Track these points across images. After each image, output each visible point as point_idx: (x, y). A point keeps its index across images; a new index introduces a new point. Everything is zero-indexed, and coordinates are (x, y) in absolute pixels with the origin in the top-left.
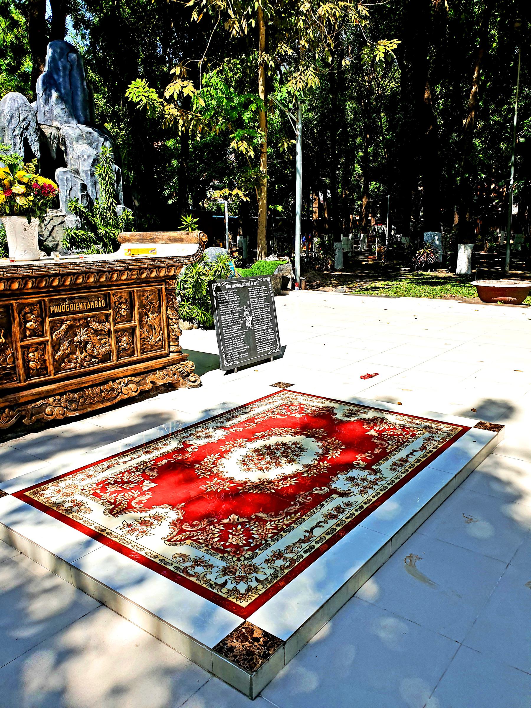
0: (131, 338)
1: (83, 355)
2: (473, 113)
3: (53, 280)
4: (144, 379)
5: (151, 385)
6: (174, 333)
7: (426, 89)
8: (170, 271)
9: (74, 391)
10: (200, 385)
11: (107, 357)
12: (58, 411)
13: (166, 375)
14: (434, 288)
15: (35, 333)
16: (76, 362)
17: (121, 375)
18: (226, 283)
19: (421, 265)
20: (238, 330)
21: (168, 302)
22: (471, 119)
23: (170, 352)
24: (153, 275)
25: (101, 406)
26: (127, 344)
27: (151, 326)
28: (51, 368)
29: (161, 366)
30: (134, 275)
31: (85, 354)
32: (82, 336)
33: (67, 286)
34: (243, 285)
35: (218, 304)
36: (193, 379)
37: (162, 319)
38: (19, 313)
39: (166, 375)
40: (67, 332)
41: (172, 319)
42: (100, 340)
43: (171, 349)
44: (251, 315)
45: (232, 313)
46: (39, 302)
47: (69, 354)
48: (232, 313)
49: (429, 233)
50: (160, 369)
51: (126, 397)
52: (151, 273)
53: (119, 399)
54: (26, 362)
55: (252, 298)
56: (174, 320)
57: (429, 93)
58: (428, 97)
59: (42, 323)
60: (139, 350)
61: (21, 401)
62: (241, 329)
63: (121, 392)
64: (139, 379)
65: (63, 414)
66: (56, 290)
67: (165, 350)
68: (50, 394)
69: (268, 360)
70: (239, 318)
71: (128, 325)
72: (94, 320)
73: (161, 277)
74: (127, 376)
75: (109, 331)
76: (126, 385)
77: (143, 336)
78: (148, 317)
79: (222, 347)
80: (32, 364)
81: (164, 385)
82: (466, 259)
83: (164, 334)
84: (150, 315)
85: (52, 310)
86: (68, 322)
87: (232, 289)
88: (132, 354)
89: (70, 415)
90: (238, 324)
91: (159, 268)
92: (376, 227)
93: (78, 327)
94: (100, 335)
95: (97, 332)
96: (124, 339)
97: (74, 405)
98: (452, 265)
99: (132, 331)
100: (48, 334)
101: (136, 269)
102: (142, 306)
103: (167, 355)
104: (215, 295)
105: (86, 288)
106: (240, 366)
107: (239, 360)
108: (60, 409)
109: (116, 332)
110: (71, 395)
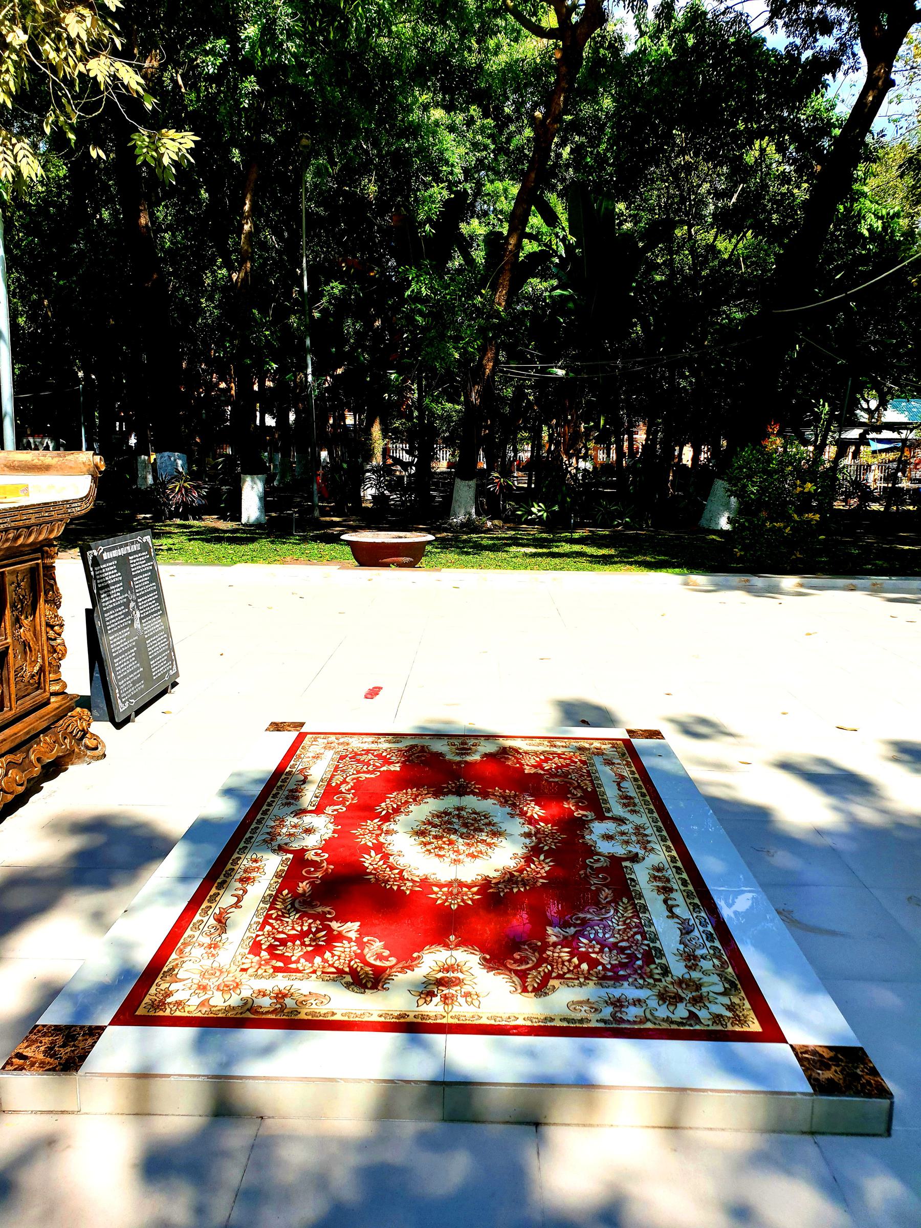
2: (249, 265)
4: (27, 756)
7: (141, 211)
10: (104, 755)
14: (251, 546)
19: (177, 508)
21: (46, 594)
22: (246, 273)
37: (38, 628)
41: (52, 627)
49: (166, 454)
50: (45, 731)
56: (56, 628)
57: (147, 217)
58: (147, 224)
60: (13, 696)
67: (45, 691)
76: (6, 774)
82: (257, 500)
92: (31, 440)
98: (233, 509)
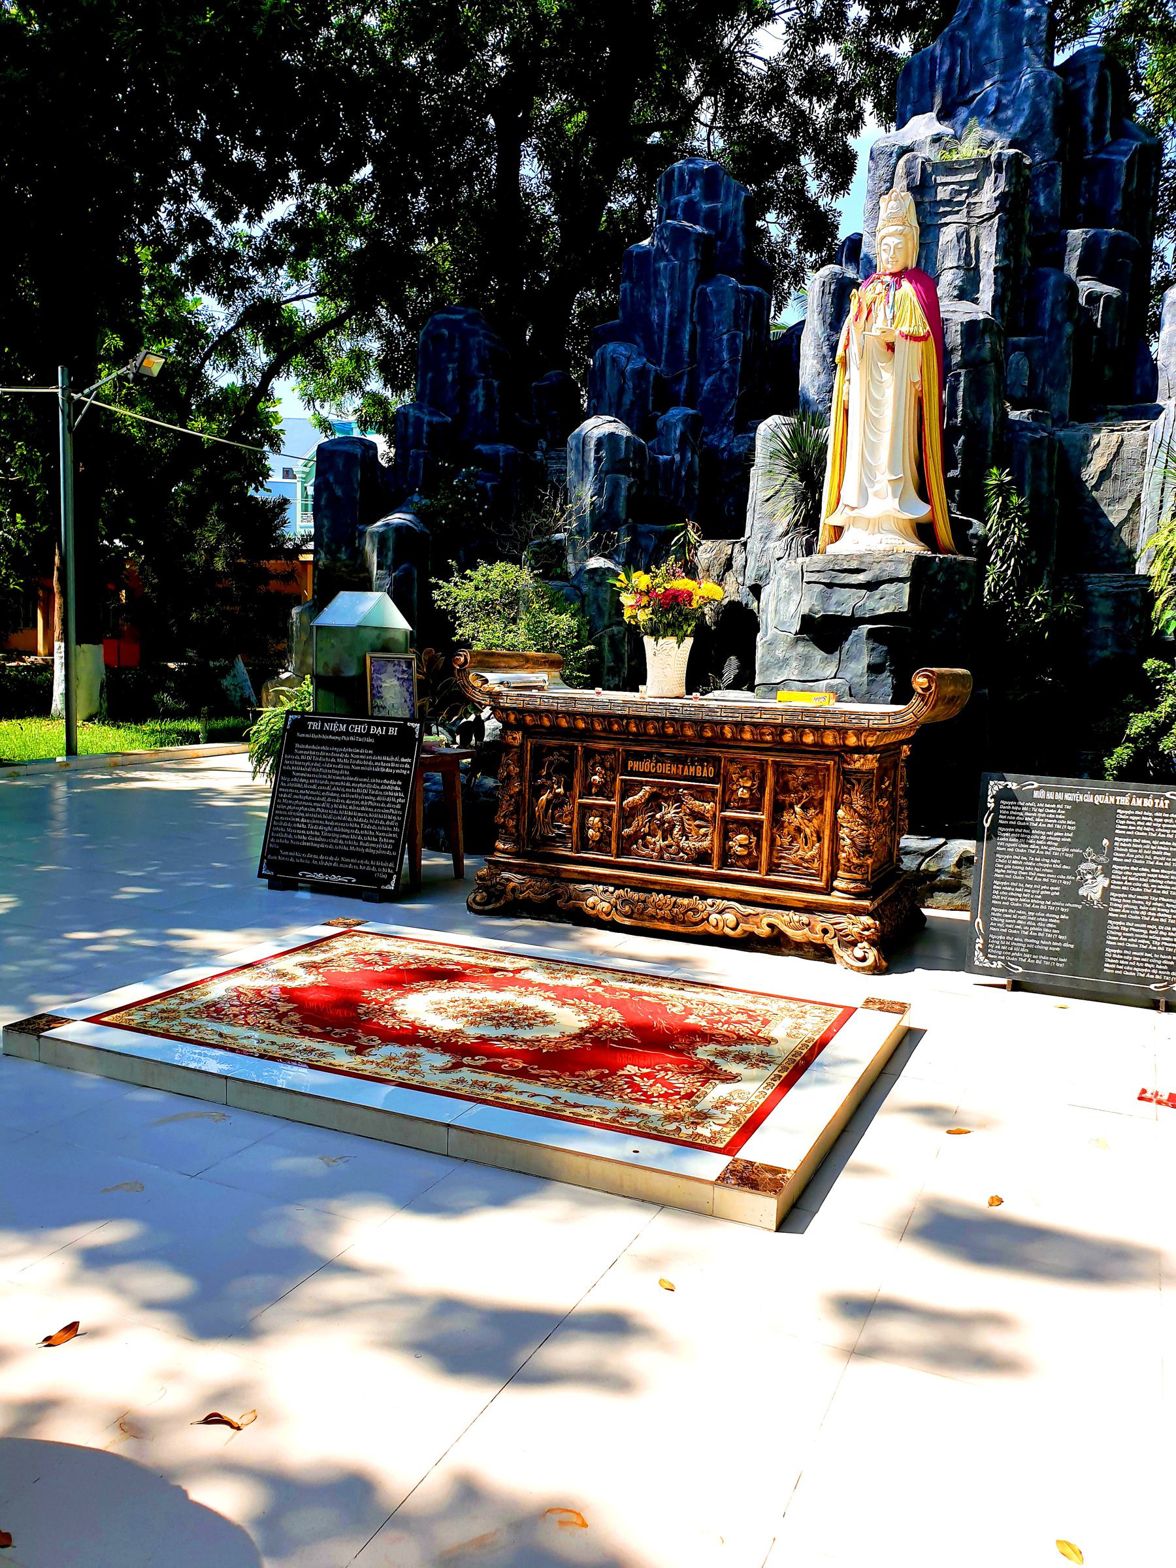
0: (754, 839)
1: (663, 844)
3: (628, 724)
5: (768, 929)
6: (844, 855)
8: (844, 739)
9: (634, 889)
11: (702, 857)
12: (605, 906)
13: (808, 925)
15: (604, 790)
16: (653, 850)
17: (718, 893)
18: (1036, 785)
20: (1045, 898)
23: (834, 889)
24: (809, 739)
25: (667, 926)
26: (740, 846)
27: (799, 830)
28: (614, 845)
29: (801, 905)
30: (764, 734)
31: (669, 841)
32: (669, 812)
33: (650, 735)
34: (1098, 799)
35: (995, 825)
36: (858, 952)
38: (586, 761)
39: (808, 925)
40: (648, 801)
42: (700, 827)
43: (835, 883)
44: (1107, 872)
45: (1034, 856)
46: (613, 751)
47: (645, 835)
48: (1034, 856)
50: (797, 910)
51: (712, 930)
52: (801, 736)
53: (700, 928)
54: (583, 827)
55: (1120, 836)
59: (614, 779)
61: (564, 875)
62: (1056, 899)
63: (707, 919)
64: (749, 910)
65: (608, 914)
66: (638, 738)
68: (603, 881)
69: (1155, 1006)
70: (1058, 872)
71: (748, 816)
72: (691, 795)
73: (828, 746)
74: (729, 900)
75: (714, 815)
76: (721, 912)
77: (778, 841)
78: (795, 812)
79: (978, 920)
80: (591, 832)
81: (811, 944)
83: (821, 849)
84: (797, 809)
85: (629, 766)
86: (647, 788)
87: (1056, 802)
88: (754, 867)
89: (619, 919)
90: (1050, 884)
91: (816, 729)
93: (666, 799)
94: (700, 819)
95: (695, 815)
96: (738, 837)
97: (627, 908)
99: (754, 827)
100: (617, 796)
101: (764, 725)
102: (782, 787)
103: (829, 889)
104: (991, 805)
105: (683, 743)
106: (1028, 980)
107: (1026, 966)
108: (606, 905)
109: (725, 820)
110: (631, 893)
